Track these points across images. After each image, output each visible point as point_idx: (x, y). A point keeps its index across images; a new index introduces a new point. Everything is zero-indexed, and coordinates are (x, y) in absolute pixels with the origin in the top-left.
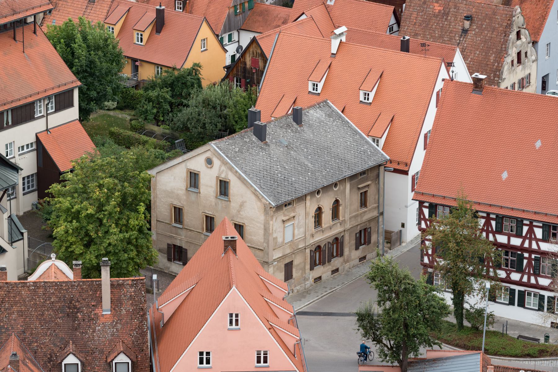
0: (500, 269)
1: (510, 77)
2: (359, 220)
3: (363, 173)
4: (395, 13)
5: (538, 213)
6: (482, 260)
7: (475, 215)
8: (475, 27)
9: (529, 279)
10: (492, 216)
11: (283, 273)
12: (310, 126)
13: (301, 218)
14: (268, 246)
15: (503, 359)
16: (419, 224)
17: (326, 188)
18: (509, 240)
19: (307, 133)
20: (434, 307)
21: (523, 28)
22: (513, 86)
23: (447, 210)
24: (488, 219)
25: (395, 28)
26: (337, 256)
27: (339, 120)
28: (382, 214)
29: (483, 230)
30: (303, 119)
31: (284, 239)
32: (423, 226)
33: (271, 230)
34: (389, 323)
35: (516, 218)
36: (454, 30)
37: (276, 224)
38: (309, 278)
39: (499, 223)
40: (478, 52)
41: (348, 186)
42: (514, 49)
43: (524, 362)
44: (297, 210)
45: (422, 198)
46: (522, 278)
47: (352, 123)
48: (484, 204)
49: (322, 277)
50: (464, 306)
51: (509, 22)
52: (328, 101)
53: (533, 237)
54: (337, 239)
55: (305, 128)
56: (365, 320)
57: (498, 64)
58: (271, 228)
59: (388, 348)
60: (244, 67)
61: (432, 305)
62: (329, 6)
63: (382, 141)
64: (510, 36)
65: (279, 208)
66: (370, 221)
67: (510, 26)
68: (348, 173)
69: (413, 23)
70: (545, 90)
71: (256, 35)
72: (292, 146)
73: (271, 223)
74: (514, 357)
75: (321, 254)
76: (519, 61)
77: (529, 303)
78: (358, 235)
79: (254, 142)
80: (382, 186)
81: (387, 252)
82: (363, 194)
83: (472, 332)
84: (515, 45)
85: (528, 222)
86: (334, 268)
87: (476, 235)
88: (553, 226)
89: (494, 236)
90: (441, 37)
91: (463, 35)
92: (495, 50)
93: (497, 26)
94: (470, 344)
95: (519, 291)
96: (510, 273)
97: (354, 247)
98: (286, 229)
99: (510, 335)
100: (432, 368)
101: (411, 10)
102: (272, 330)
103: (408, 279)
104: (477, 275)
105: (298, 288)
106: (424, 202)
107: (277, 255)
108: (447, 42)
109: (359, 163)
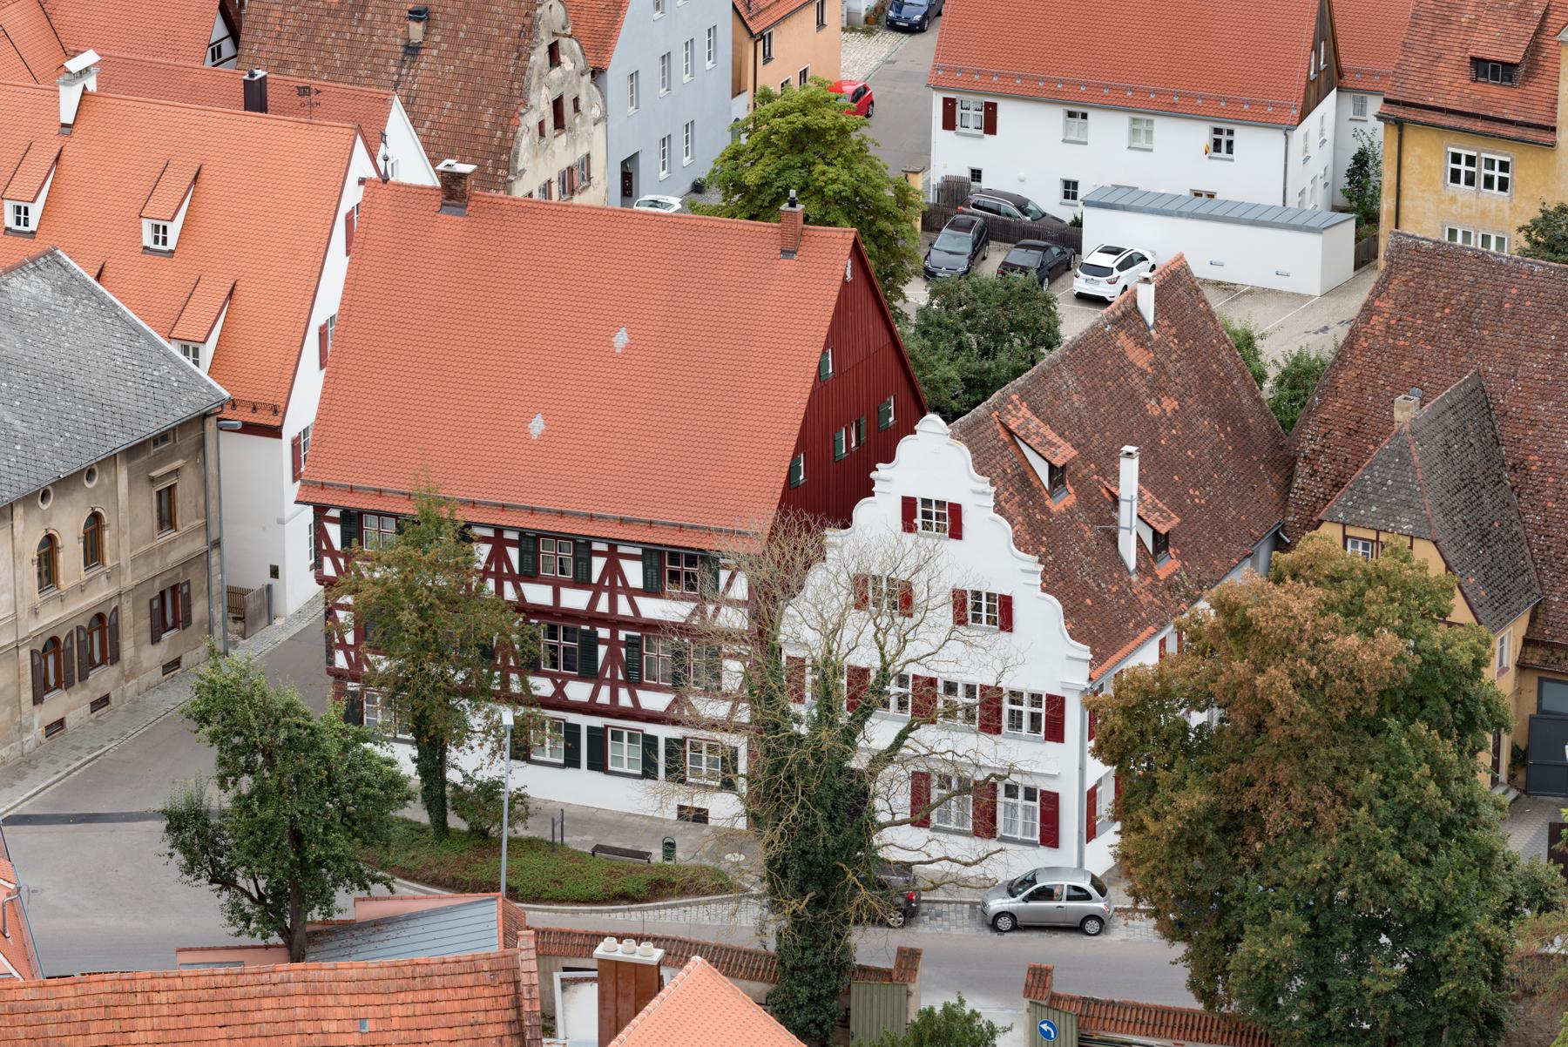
0: (537, 672)
1: (537, 167)
2: (157, 564)
3: (162, 438)
5: (630, 522)
6: (488, 653)
7: (464, 535)
8: (438, 38)
9: (614, 695)
10: (508, 535)
15: (556, 911)
16: (318, 565)
17: (65, 484)
20: (369, 785)
21: (565, 36)
22: (546, 189)
23: (390, 525)
24: (499, 544)
25: (227, 49)
26: (103, 662)
27: (90, 299)
28: (217, 544)
32: (329, 569)
34: (252, 833)
38: (32, 725)
39: (528, 552)
40: (449, 105)
41: (123, 475)
42: (545, 91)
45: (322, 498)
46: (595, 693)
51: (527, 21)
52: (59, 252)
54: (100, 617)
56: (191, 833)
57: (505, 132)
59: (252, 899)
61: (362, 779)
64: (532, 58)
66: (186, 564)
68: (123, 441)
69: (274, 35)
70: (630, 195)
76: (559, 123)
77: (618, 760)
78: (156, 604)
81: (235, 644)
82: (165, 495)
83: (472, 842)
84: (545, 80)
85: (603, 547)
86: (98, 696)
87: (469, 586)
88: (671, 554)
89: (517, 588)
90: (349, 67)
93: (496, 32)
94: (467, 877)
95: (590, 729)
97: (147, 636)
100: (372, 946)
104: (477, 692)
106: (326, 508)
108: (366, 81)
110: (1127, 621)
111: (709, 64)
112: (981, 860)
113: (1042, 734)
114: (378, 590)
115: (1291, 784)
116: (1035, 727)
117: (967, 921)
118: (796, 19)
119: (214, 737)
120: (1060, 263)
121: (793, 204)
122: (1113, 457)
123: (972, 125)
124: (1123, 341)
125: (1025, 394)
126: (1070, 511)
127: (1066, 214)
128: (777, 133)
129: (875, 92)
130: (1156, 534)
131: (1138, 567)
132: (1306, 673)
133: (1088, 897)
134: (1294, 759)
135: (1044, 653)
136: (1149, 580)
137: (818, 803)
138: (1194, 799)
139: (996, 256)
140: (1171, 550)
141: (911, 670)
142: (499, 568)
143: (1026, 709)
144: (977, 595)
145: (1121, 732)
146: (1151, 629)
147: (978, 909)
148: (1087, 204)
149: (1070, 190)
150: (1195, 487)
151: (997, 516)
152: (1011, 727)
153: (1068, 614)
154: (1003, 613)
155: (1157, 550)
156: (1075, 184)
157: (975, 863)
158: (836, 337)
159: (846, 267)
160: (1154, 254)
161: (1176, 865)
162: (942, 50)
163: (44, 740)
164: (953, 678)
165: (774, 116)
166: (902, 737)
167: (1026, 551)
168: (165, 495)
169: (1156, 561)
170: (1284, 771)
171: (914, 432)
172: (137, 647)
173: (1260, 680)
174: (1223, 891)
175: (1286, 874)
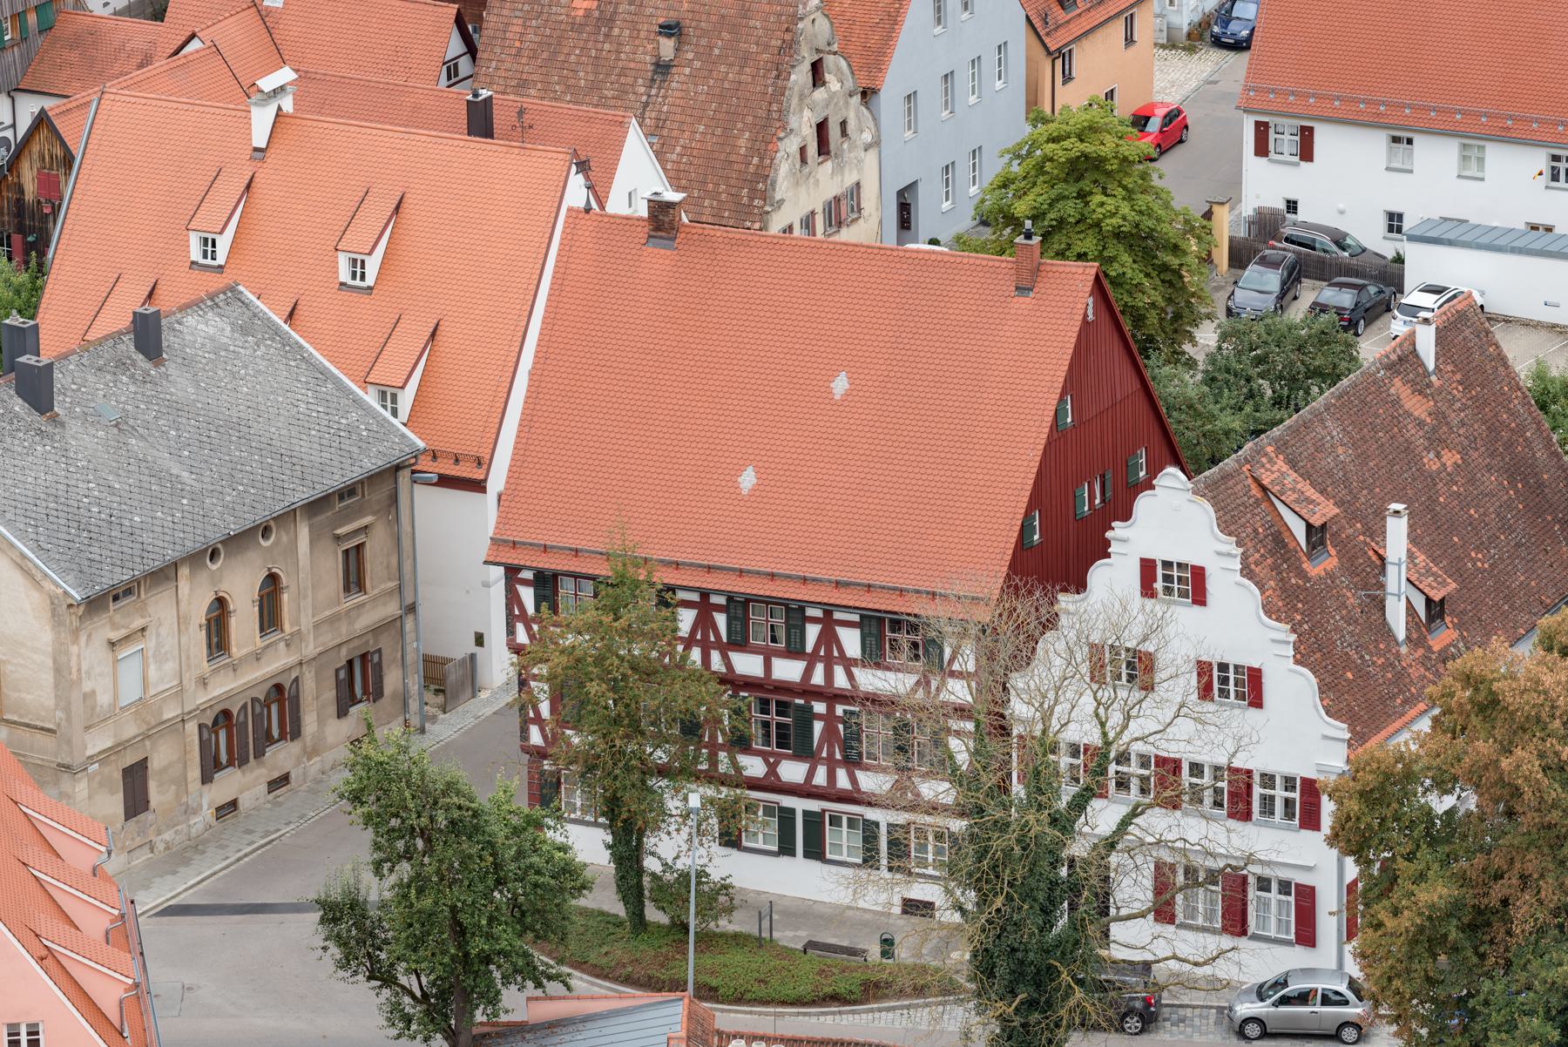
0: (747, 749)
1: (798, 196)
2: (344, 630)
3: (348, 491)
4: (460, 22)
5: (847, 584)
6: (691, 729)
7: (666, 598)
8: (690, 56)
9: (831, 776)
10: (715, 599)
11: (121, 795)
12: (187, 363)
13: (163, 631)
14: (69, 719)
15: (760, 1014)
16: (511, 631)
17: (238, 542)
18: (768, 666)
19: (178, 382)
20: (538, 872)
21: (829, 53)
22: (808, 222)
23: (589, 586)
24: (704, 607)
25: (465, 66)
26: (282, 737)
27: (273, 340)
28: (412, 609)
29: (689, 643)
30: (165, 344)
31: (116, 697)
32: (522, 637)
33: (74, 670)
34: (411, 925)
35: (785, 603)
36: (632, 65)
37: (90, 653)
38: (201, 806)
39: (736, 618)
40: (702, 128)
41: (304, 532)
42: (807, 113)
43: (822, 1019)
44: (151, 610)
45: (514, 558)
46: (811, 774)
47: (311, 349)
48: (691, 565)
49: (240, 802)
50: (645, 864)
51: (788, 37)
52: (241, 288)
53: (836, 654)
54: (278, 688)
55: (172, 368)
56: (345, 921)
57: (762, 159)
58: (74, 663)
59: (413, 997)
60: (18, 200)
61: (531, 866)
62: (269, 10)
63: (406, 399)
64: (793, 77)
65: (95, 605)
67: (789, 47)
68: (303, 495)
69: (514, 51)
70: (909, 228)
71: (48, 103)
72: (131, 422)
73: (74, 649)
74: (792, 1004)
75: (233, 736)
77: (837, 847)
78: (342, 674)
79: (17, 415)
80: (409, 529)
81: (433, 719)
82: (352, 556)
84: (808, 101)
85: (818, 613)
86: (276, 775)
87: (672, 655)
88: (891, 621)
89: (725, 658)
90: (594, 87)
91: (658, 78)
92: (750, 119)
93: (754, 48)
94: (664, 975)
95: (805, 813)
96: (777, 763)
97: (333, 709)
98: (122, 667)
99: (783, 943)
101: (505, 12)
102: (49, 962)
103: (458, 793)
105: (167, 836)
106: (518, 569)
107: (99, 742)
108: (613, 102)
109: (335, 463)
110: (1393, 697)
111: (999, 84)
112: (1214, 959)
113: (1297, 822)
114: (564, 659)
115: (1542, 876)
116: (1289, 815)
117: (1212, 1028)
118: (1100, 35)
119: (368, 819)
120: (1379, 303)
121: (1028, 236)
122: (1380, 515)
123: (1286, 152)
124: (1398, 387)
125: (1281, 446)
126: (1330, 575)
127: (1387, 248)
128: (1051, 160)
129: (1191, 117)
130: (1429, 601)
131: (1408, 638)
132: (1557, 754)
133: (1346, 1003)
134: (1546, 850)
135: (1297, 734)
136: (1421, 652)
137: (1028, 895)
138: (1436, 893)
139: (1310, 293)
140: (1448, 619)
141: (1138, 747)
142: (705, 636)
143: (1279, 793)
144: (1223, 667)
145: (1358, 819)
146: (1422, 706)
147: (1225, 1012)
148: (1412, 238)
149: (1394, 222)
150: (1478, 549)
151: (1246, 581)
152: (1262, 813)
153: (1324, 689)
154: (1252, 688)
155: (1431, 618)
156: (1400, 216)
157: (1205, 963)
158: (1075, 383)
159: (1083, 302)
160: (1482, 294)
161: (1416, 966)
162: (1252, 72)
163: (214, 823)
164: (1198, 758)
165: (1048, 141)
166: (1125, 823)
167: (1278, 620)
168: (352, 556)
169: (1430, 631)
170: (1532, 863)
171: (1152, 487)
172: (321, 722)
173: (1505, 763)
174: (1470, 995)
175: (1536, 976)
